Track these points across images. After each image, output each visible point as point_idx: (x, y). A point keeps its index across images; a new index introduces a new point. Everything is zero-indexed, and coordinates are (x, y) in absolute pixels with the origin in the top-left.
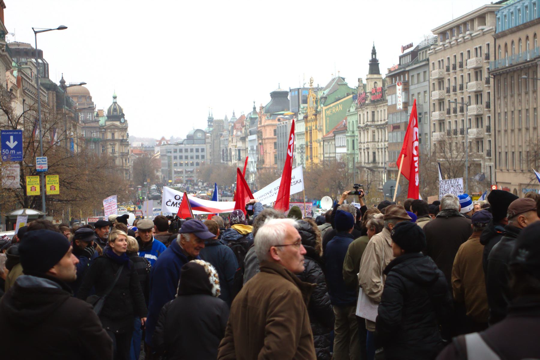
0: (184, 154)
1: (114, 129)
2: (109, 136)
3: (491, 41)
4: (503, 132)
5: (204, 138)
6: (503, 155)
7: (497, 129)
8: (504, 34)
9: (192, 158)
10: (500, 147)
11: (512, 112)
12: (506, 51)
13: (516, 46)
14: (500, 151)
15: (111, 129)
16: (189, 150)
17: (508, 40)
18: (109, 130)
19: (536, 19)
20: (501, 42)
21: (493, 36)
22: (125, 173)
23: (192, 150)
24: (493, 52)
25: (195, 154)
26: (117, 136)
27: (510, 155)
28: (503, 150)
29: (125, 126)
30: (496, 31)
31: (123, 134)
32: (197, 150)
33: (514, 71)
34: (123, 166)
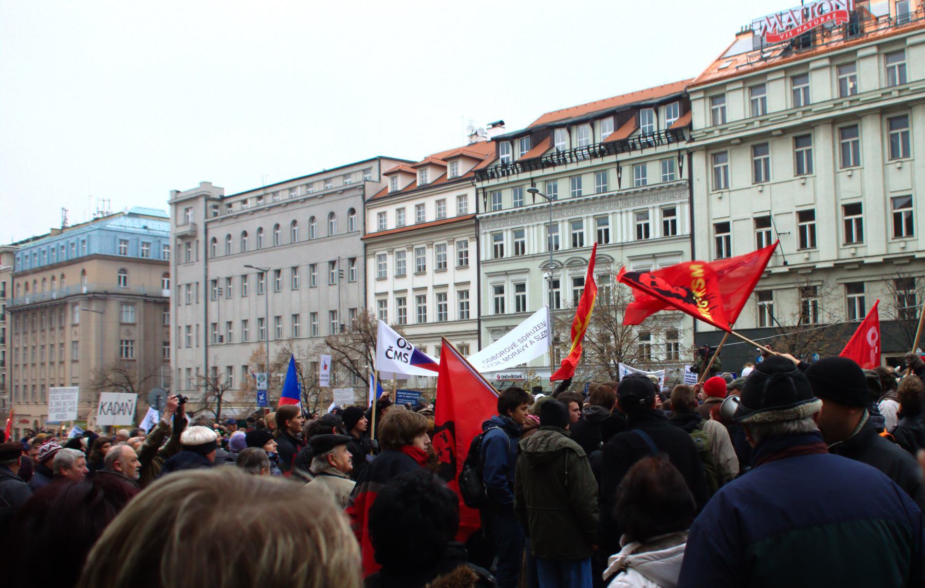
3: (8, 280)
4: (21, 366)
6: (21, 389)
7: (14, 363)
8: (24, 274)
10: (17, 381)
11: (34, 347)
12: (27, 289)
13: (39, 286)
14: (17, 384)
17: (30, 279)
19: (65, 261)
20: (21, 281)
21: (10, 274)
24: (11, 290)
27: (30, 388)
28: (21, 384)
30: (14, 270)
33: (38, 309)
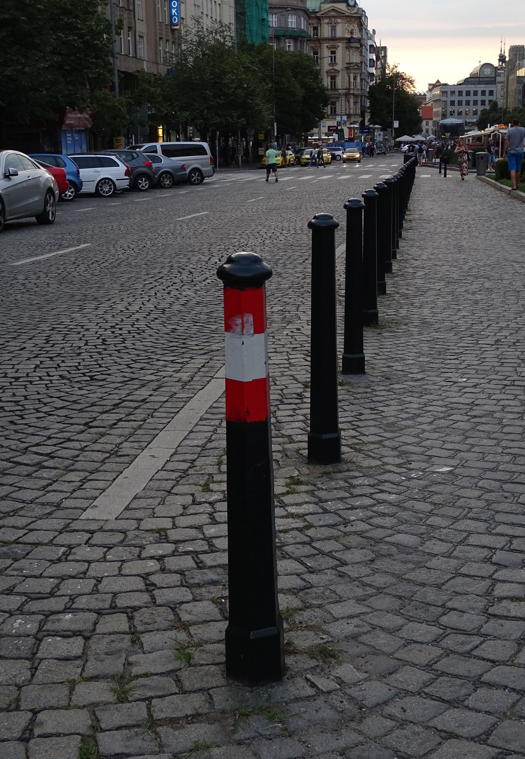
0: (464, 98)
1: (335, 17)
2: (326, 31)
5: (494, 76)
9: (475, 103)
15: (330, 17)
16: (472, 93)
18: (326, 21)
22: (352, 101)
23: (475, 93)
25: (479, 98)
26: (341, 31)
29: (355, 13)
31: (351, 27)
32: (483, 93)
34: (349, 89)
